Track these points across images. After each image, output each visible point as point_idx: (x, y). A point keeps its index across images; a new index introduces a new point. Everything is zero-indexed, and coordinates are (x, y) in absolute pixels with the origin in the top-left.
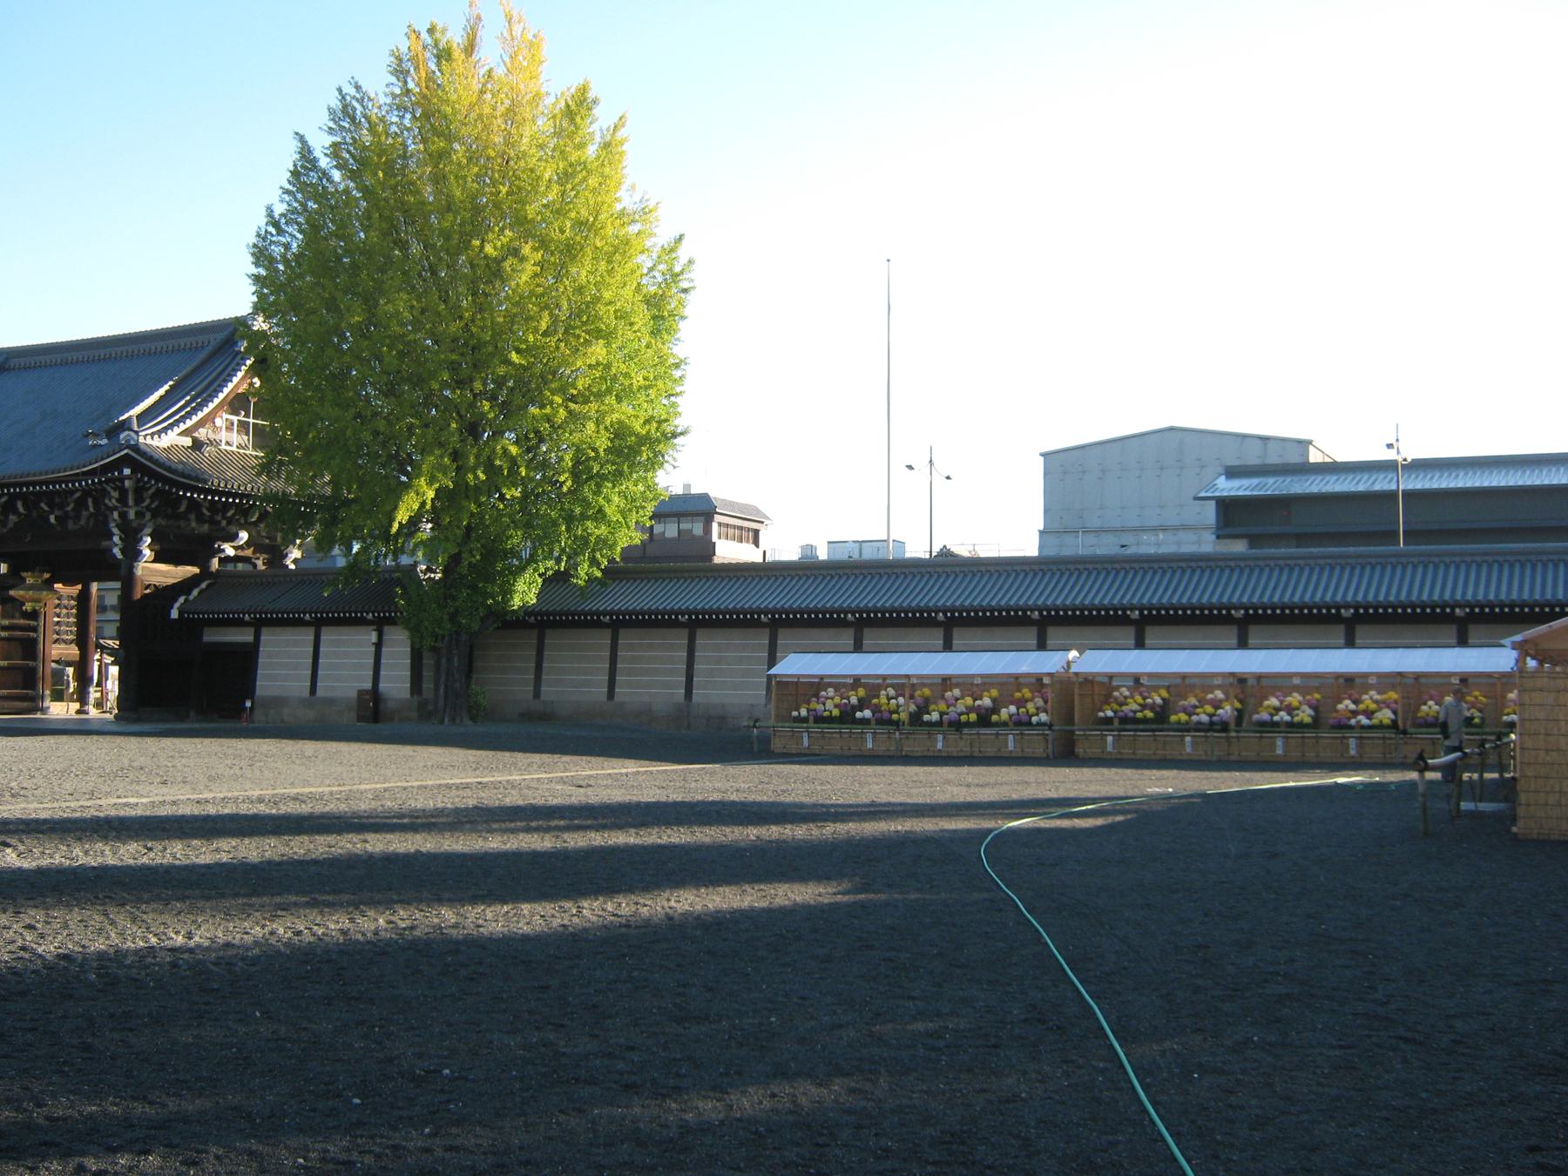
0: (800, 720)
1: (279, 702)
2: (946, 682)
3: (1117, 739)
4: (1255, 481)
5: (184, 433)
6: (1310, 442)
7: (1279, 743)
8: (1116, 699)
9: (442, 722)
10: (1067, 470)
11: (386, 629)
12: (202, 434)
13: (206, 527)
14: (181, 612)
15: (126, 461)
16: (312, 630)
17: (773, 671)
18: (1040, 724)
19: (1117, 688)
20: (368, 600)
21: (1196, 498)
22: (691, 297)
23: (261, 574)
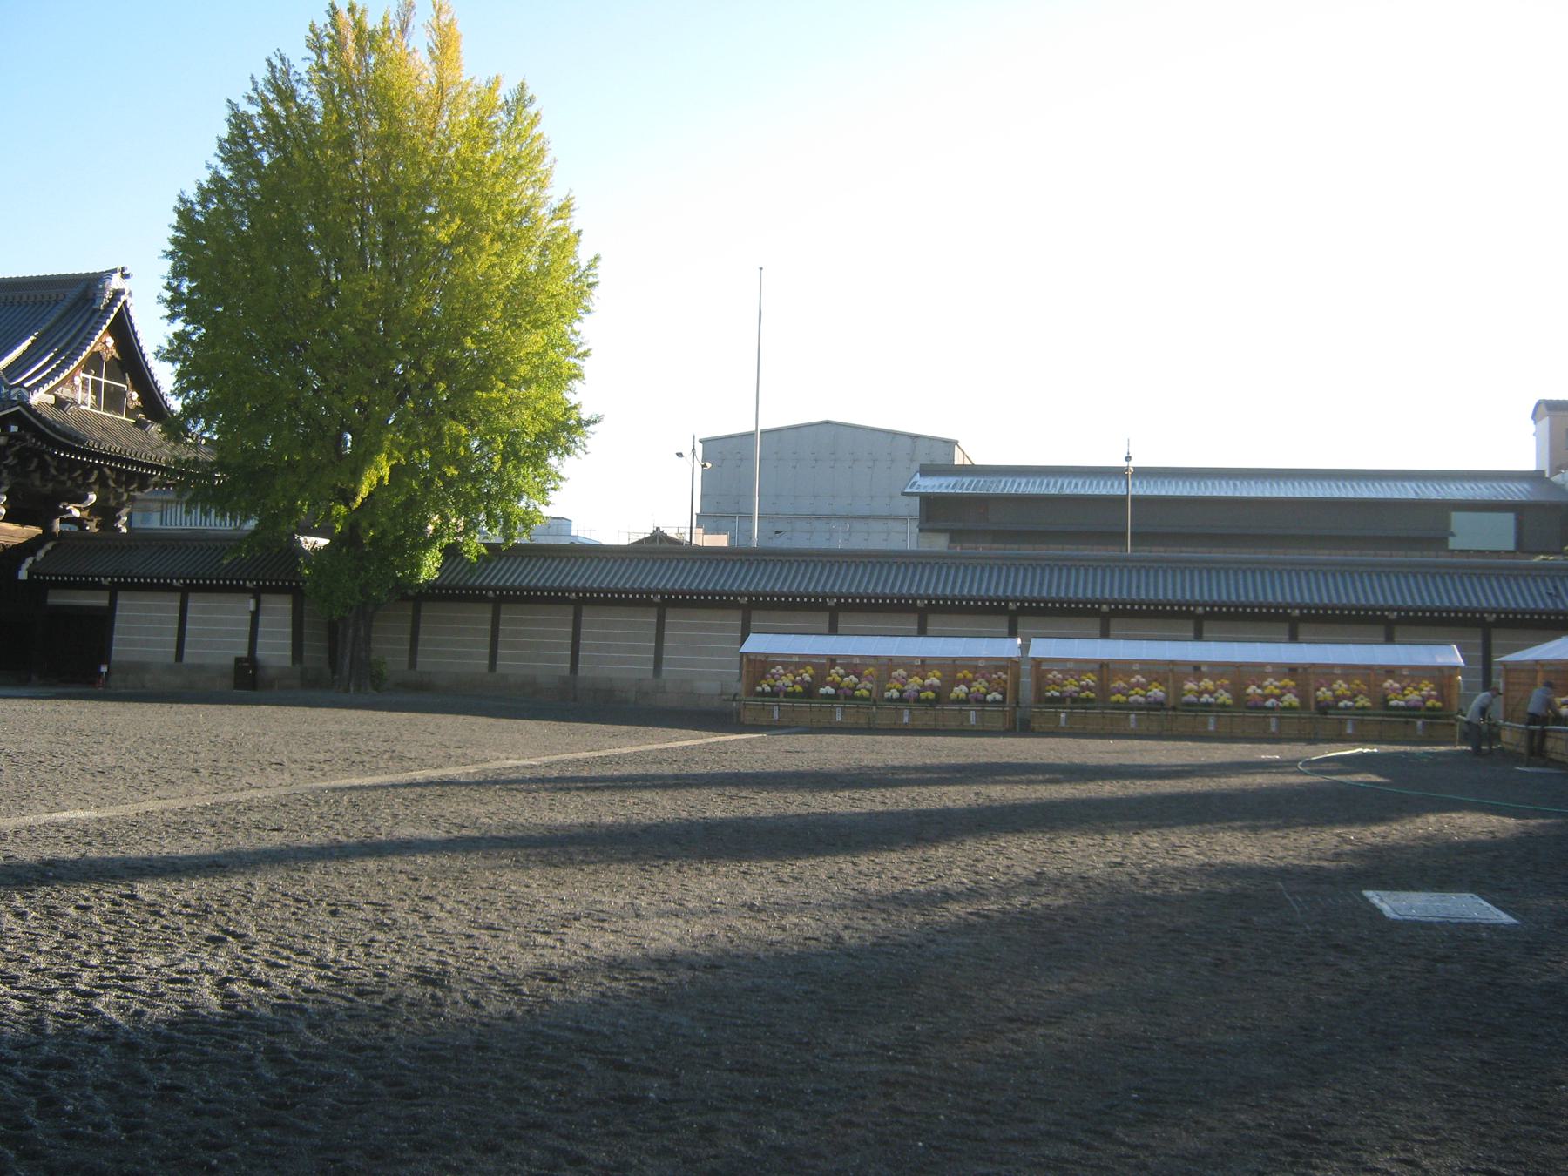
0: (763, 694)
1: (140, 667)
2: (832, 661)
3: (1070, 715)
4: (952, 480)
5: (50, 392)
6: (956, 443)
7: (1212, 720)
8: (773, 676)
9: (347, 691)
10: (725, 460)
11: (264, 597)
12: (65, 392)
13: (50, 485)
14: (30, 574)
15: (16, 418)
16: (178, 596)
17: (744, 649)
18: (994, 701)
19: (1049, 671)
20: (264, 570)
21: (904, 494)
22: (596, 291)
23: (92, 537)
